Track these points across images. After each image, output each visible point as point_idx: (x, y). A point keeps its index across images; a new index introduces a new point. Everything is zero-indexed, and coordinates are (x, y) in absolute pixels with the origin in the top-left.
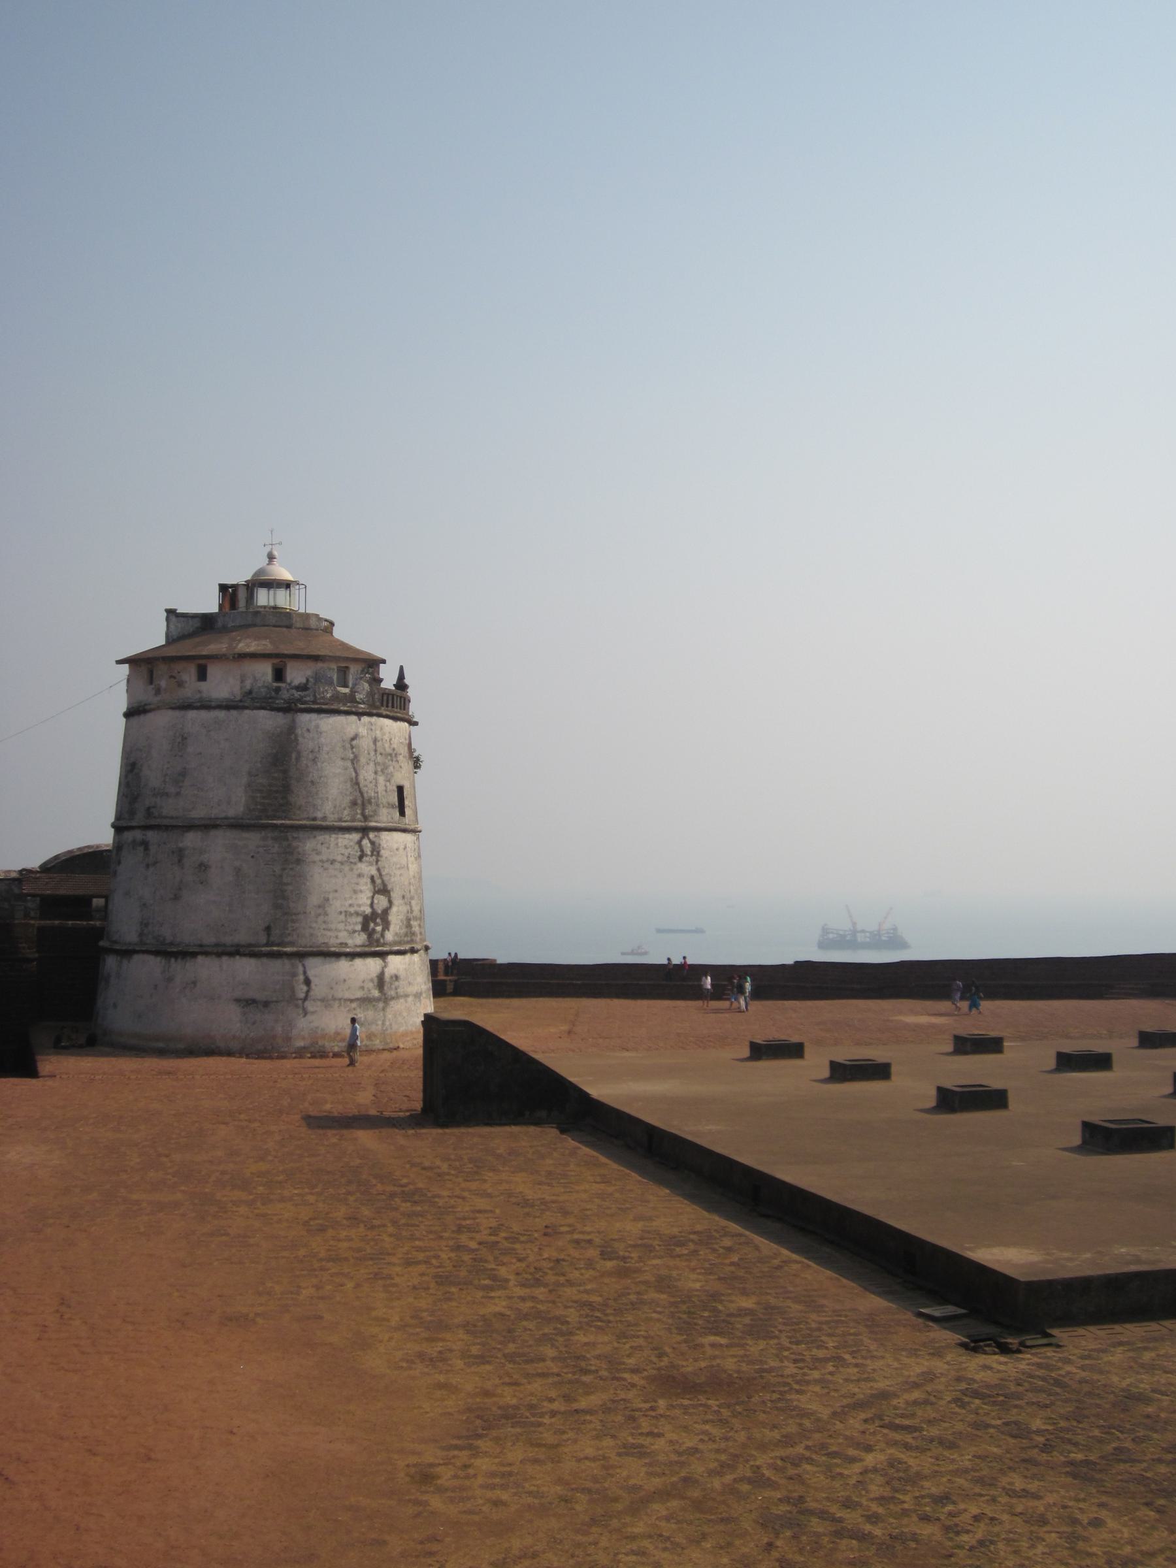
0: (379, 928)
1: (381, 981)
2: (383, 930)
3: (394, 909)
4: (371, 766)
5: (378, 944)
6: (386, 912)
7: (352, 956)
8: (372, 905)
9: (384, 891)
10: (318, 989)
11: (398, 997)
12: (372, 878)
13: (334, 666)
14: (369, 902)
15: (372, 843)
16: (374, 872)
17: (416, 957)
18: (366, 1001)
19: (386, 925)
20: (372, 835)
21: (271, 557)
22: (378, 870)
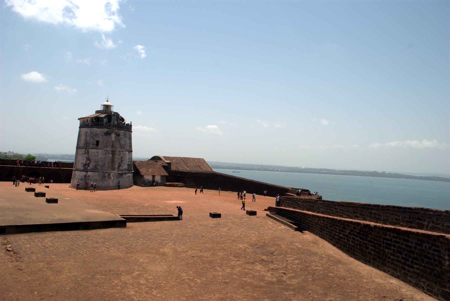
1: (85, 176)
4: (89, 137)
5: (86, 169)
7: (81, 171)
10: (76, 177)
11: (89, 180)
13: (86, 119)
17: (96, 173)
18: (82, 179)
19: (89, 166)
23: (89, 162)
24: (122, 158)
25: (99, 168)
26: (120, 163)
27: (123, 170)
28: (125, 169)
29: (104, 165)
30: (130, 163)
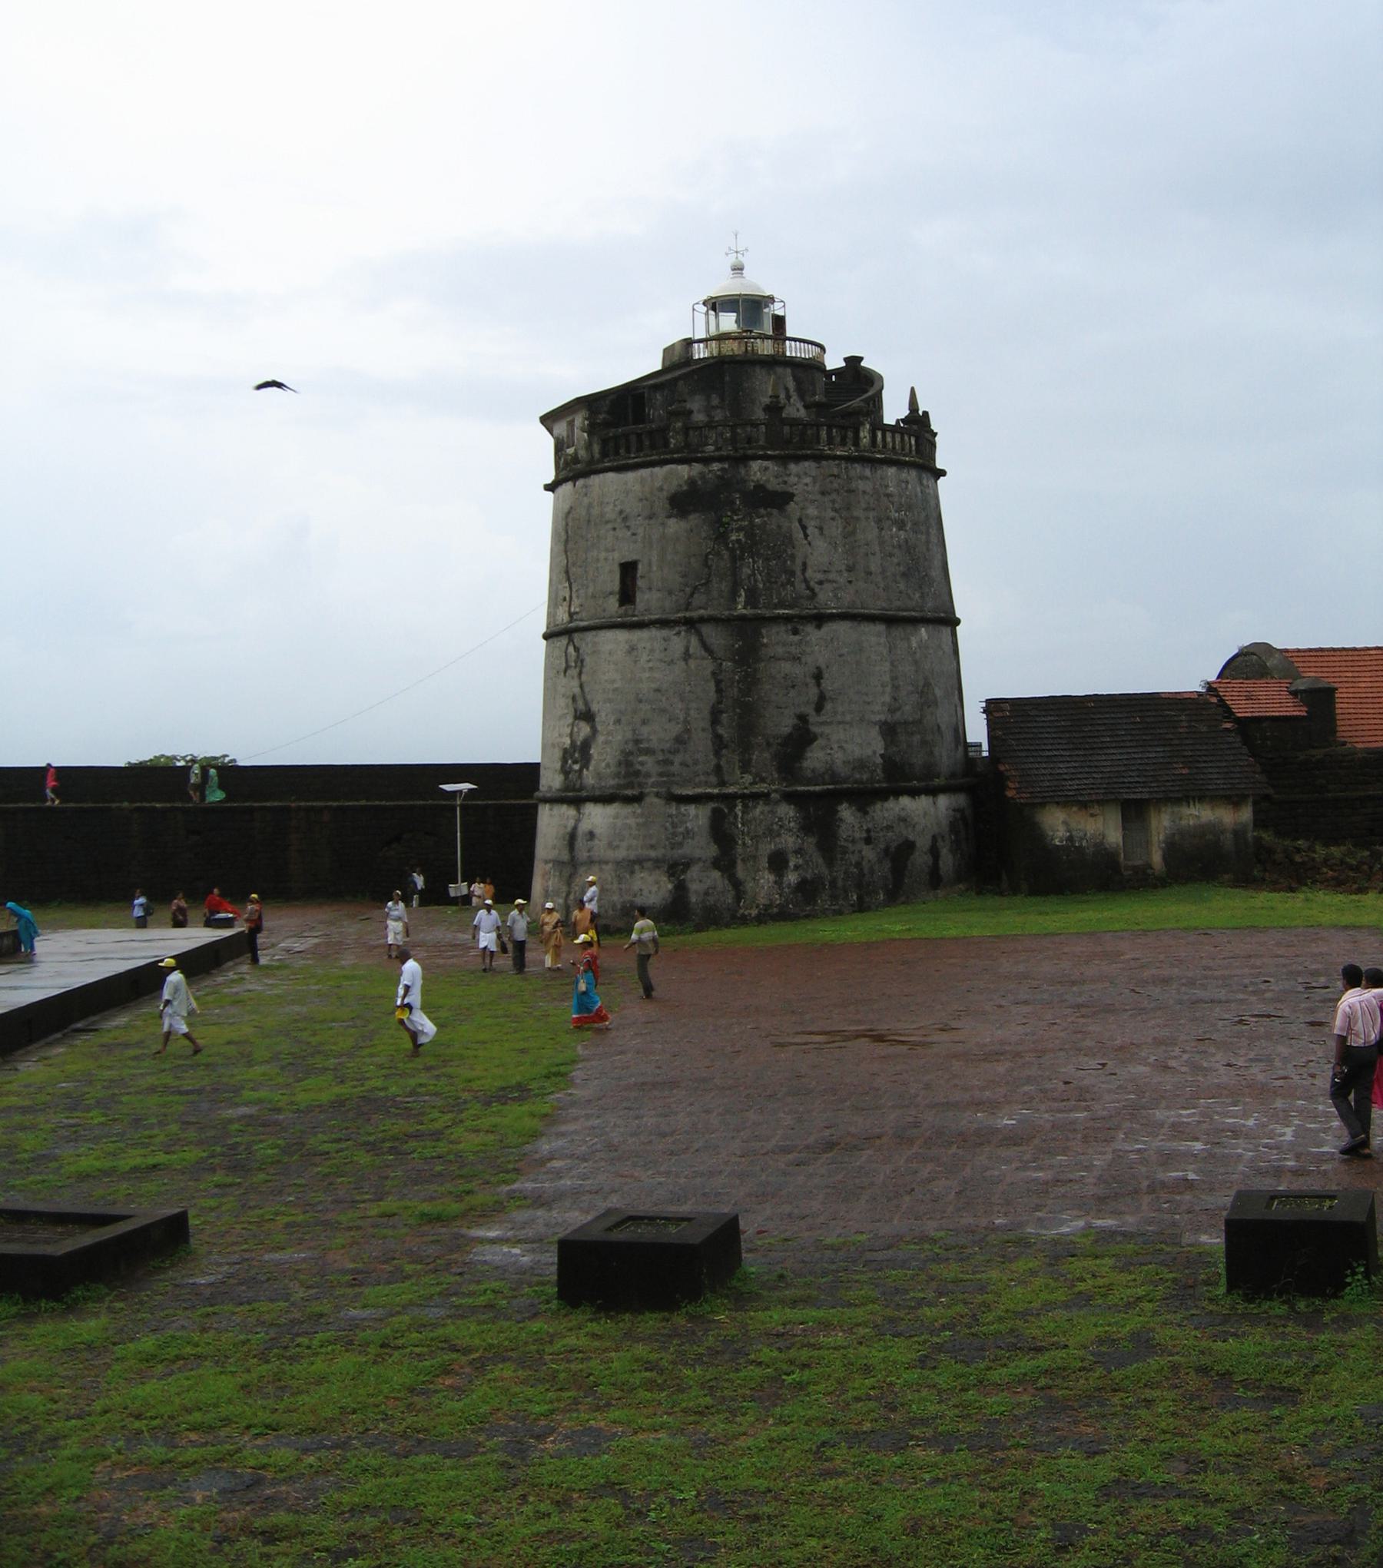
0: (576, 767)
2: (580, 771)
3: (601, 739)
6: (586, 746)
8: (571, 735)
9: (586, 716)
11: (591, 862)
12: (574, 698)
14: (568, 730)
15: (577, 649)
16: (577, 690)
20: (576, 636)
21: (738, 269)
22: (581, 686)
23: (585, 729)
24: (818, 676)
25: (648, 764)
26: (802, 718)
27: (843, 771)
28: (861, 765)
29: (679, 740)
30: (908, 711)
